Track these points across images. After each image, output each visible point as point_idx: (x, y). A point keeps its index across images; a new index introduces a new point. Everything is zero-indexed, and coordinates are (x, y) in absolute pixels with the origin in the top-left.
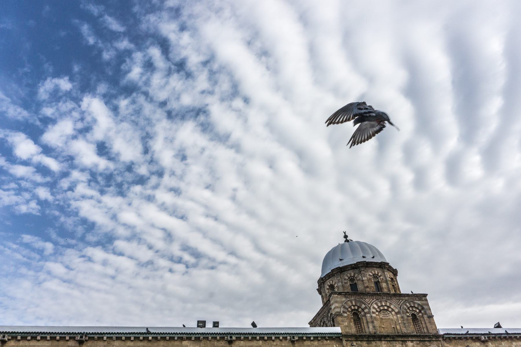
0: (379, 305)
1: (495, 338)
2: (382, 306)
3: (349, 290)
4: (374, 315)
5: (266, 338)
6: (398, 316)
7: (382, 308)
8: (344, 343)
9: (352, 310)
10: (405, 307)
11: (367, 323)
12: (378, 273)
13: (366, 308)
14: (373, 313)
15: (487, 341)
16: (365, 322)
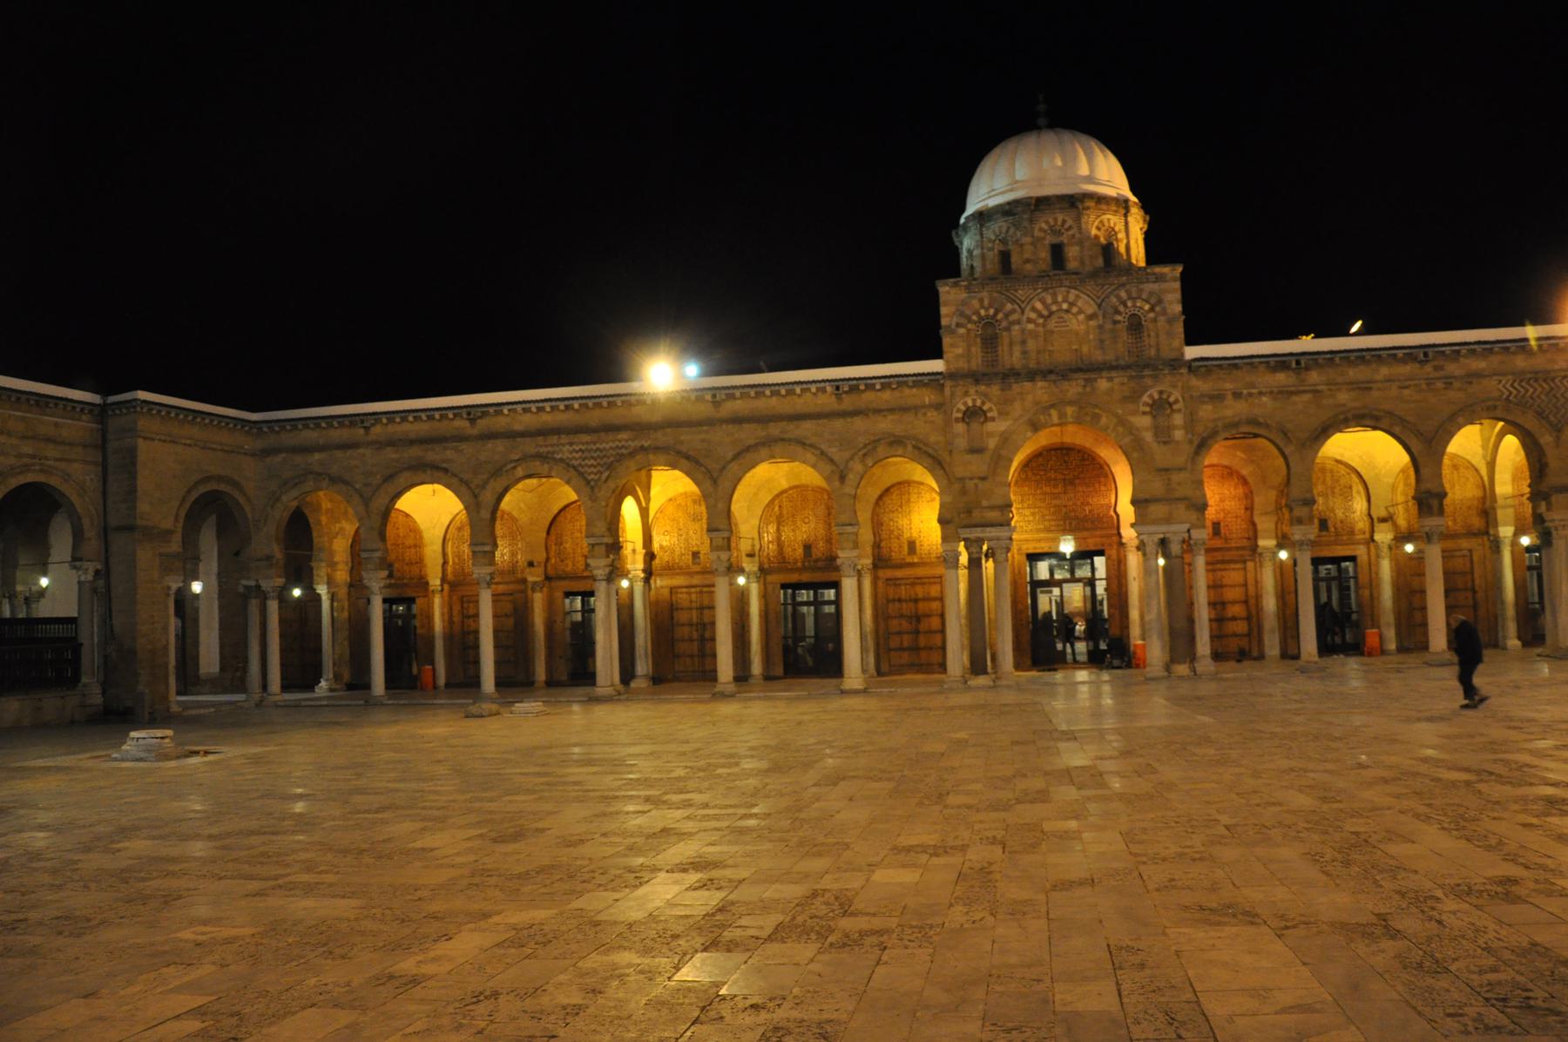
0: (1049, 300)
1: (1332, 359)
2: (1055, 302)
3: (993, 265)
4: (1031, 326)
5: (783, 392)
6: (1092, 323)
7: (1054, 308)
8: (947, 391)
9: (981, 318)
10: (1114, 300)
11: (1011, 344)
12: (1064, 222)
13: (1013, 311)
14: (1029, 321)
15: (1307, 369)
16: (1006, 341)
